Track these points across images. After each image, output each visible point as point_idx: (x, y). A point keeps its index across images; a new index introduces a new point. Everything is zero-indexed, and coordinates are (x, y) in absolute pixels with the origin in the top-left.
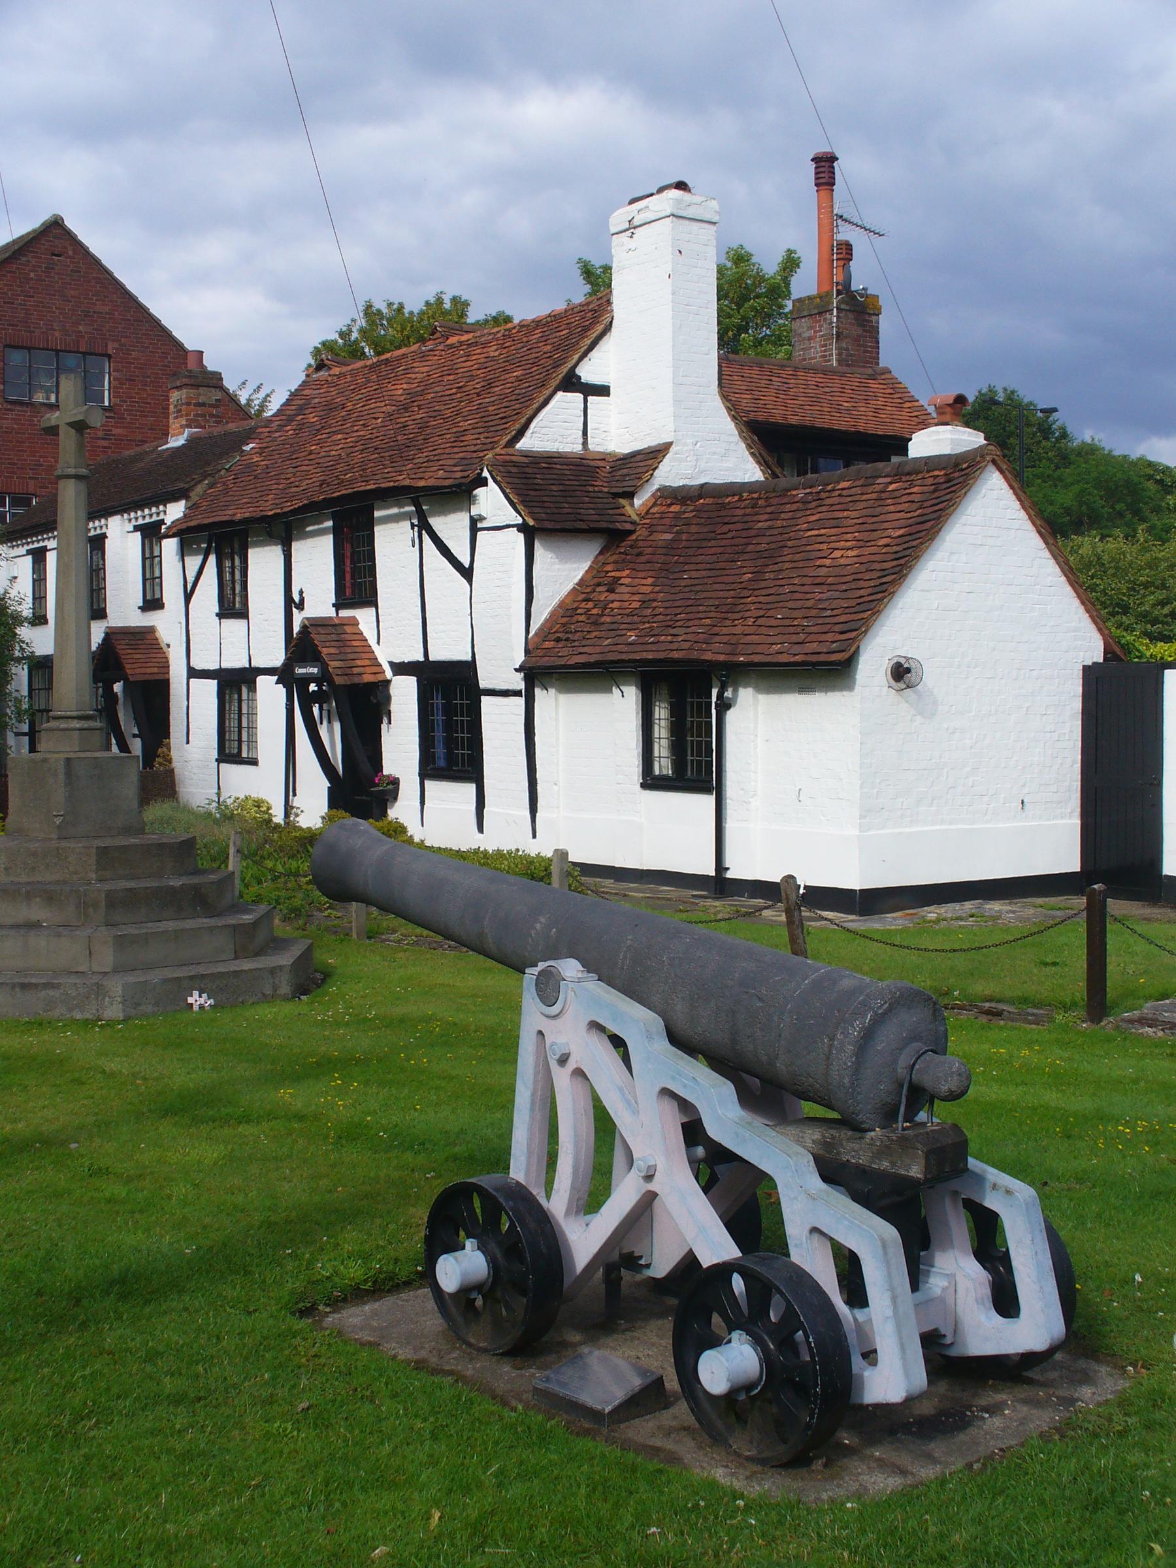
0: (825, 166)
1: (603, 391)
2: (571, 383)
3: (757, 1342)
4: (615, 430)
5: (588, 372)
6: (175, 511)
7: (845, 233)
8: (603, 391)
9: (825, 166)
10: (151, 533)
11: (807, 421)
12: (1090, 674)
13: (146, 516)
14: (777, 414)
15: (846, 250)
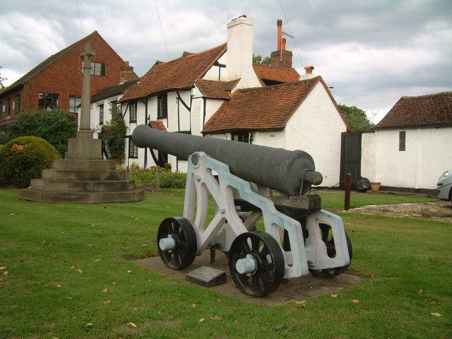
0: (280, 23)
1: (224, 66)
2: (217, 64)
3: (255, 258)
4: (226, 75)
5: (221, 61)
6: (120, 97)
7: (284, 36)
8: (224, 66)
9: (280, 23)
10: (114, 103)
11: (274, 79)
12: (343, 135)
13: (113, 99)
14: (267, 77)
15: (284, 41)
